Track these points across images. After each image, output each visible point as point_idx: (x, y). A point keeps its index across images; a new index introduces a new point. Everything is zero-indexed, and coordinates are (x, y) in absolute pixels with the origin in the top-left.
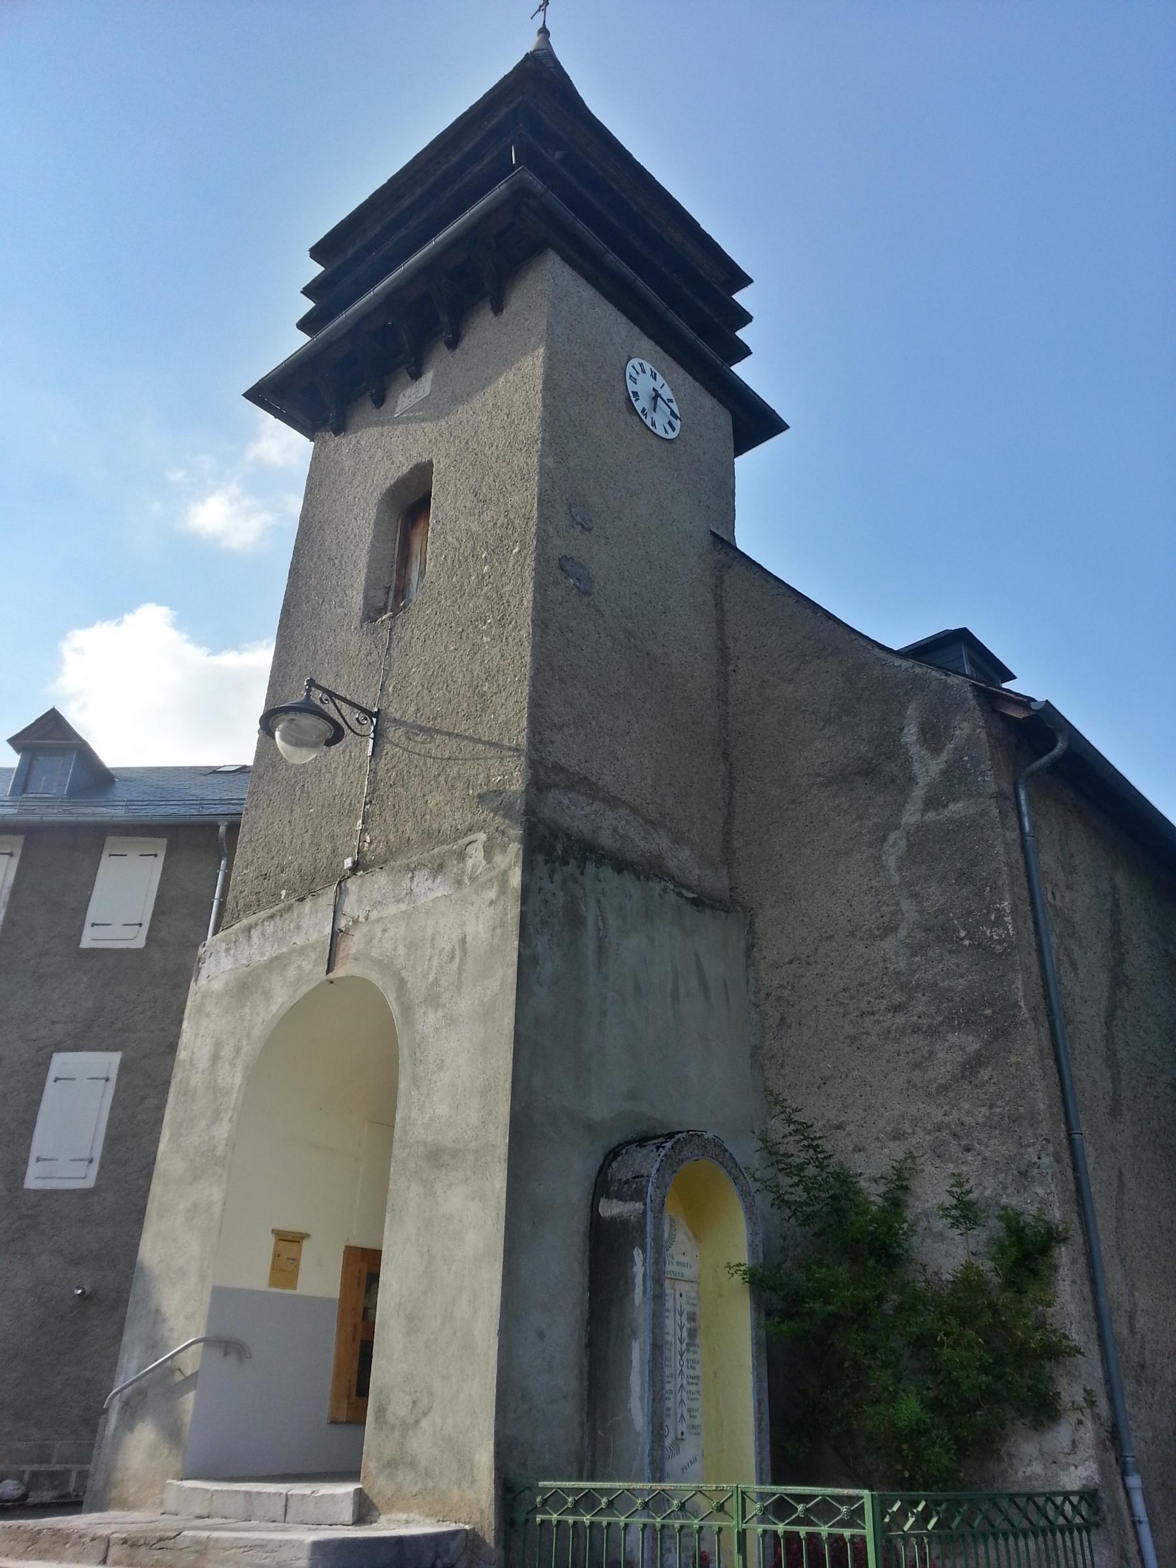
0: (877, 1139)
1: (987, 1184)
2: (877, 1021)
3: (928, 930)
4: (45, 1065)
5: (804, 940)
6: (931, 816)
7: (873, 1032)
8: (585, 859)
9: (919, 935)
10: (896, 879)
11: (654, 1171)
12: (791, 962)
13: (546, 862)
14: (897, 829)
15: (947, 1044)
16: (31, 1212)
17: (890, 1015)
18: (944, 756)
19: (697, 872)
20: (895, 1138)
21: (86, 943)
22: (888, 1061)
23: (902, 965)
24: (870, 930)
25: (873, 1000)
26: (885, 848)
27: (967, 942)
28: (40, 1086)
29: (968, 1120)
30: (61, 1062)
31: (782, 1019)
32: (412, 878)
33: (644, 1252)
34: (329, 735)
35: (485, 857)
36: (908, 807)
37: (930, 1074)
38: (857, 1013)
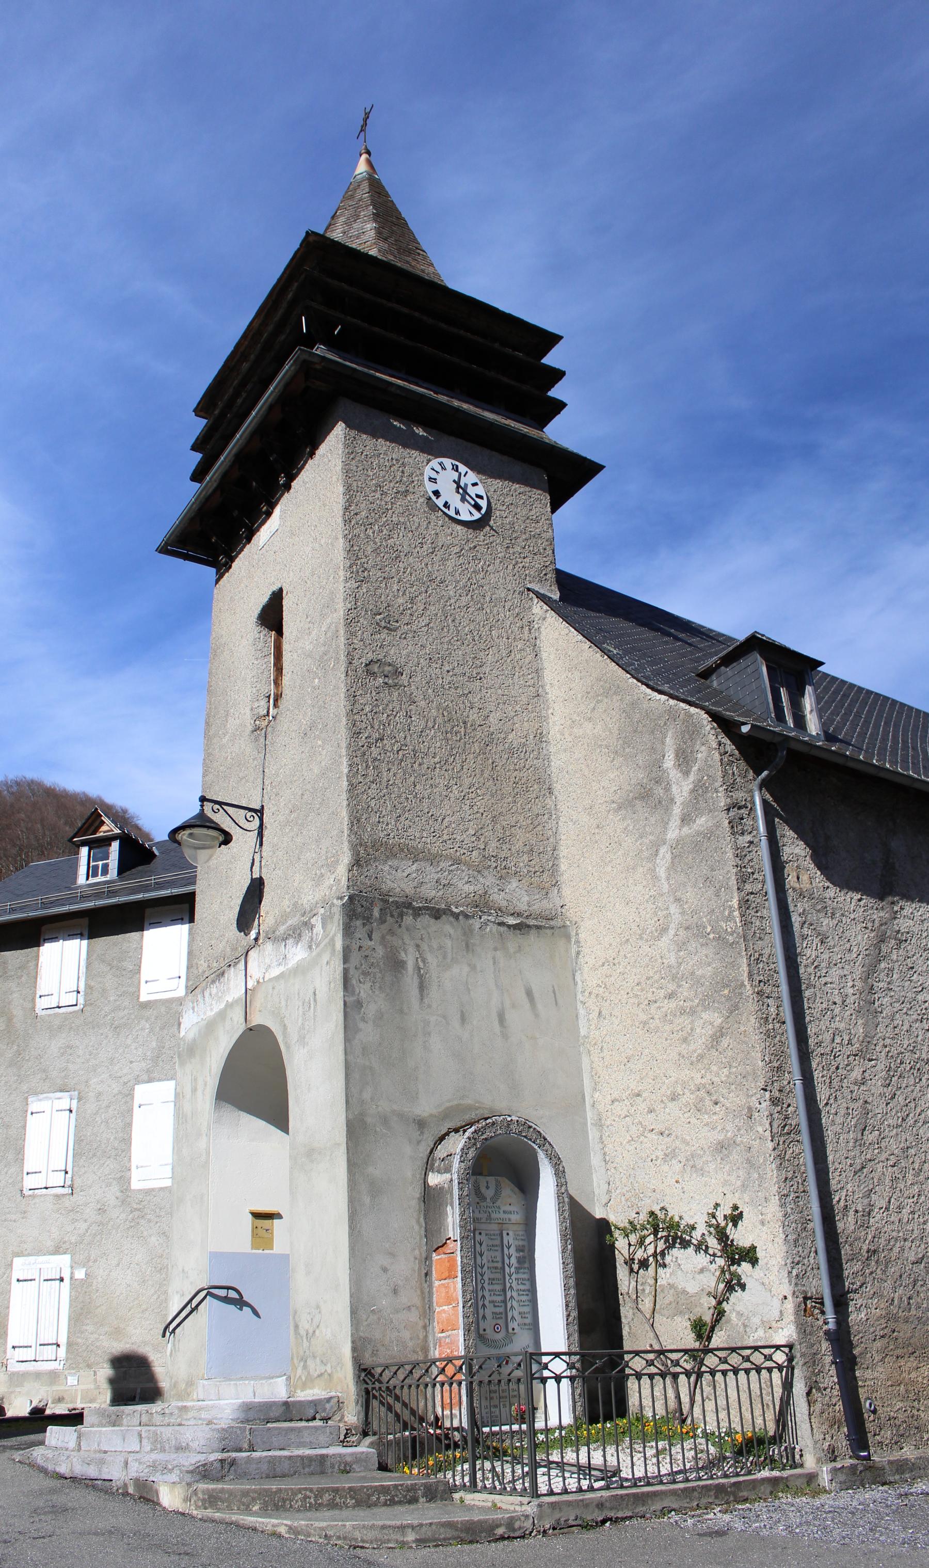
0: (662, 1101)
1: (728, 1128)
2: (659, 1008)
3: (687, 928)
4: (130, 1095)
5: (611, 945)
6: (686, 830)
7: (656, 1017)
8: (401, 915)
9: (682, 932)
10: (666, 888)
11: (458, 1150)
12: (603, 965)
13: (364, 925)
14: (665, 844)
15: (702, 1021)
16: (138, 1206)
17: (666, 1001)
18: (692, 777)
19: (526, 899)
20: (673, 1099)
21: (144, 998)
22: (666, 1040)
23: (672, 960)
24: (652, 932)
25: (655, 990)
26: (658, 861)
27: (711, 936)
28: (130, 1111)
29: (716, 1079)
30: (142, 1092)
31: (600, 1013)
32: (285, 945)
33: (452, 1208)
34: (221, 838)
35: (323, 928)
36: (671, 824)
37: (692, 1047)
38: (647, 1002)
